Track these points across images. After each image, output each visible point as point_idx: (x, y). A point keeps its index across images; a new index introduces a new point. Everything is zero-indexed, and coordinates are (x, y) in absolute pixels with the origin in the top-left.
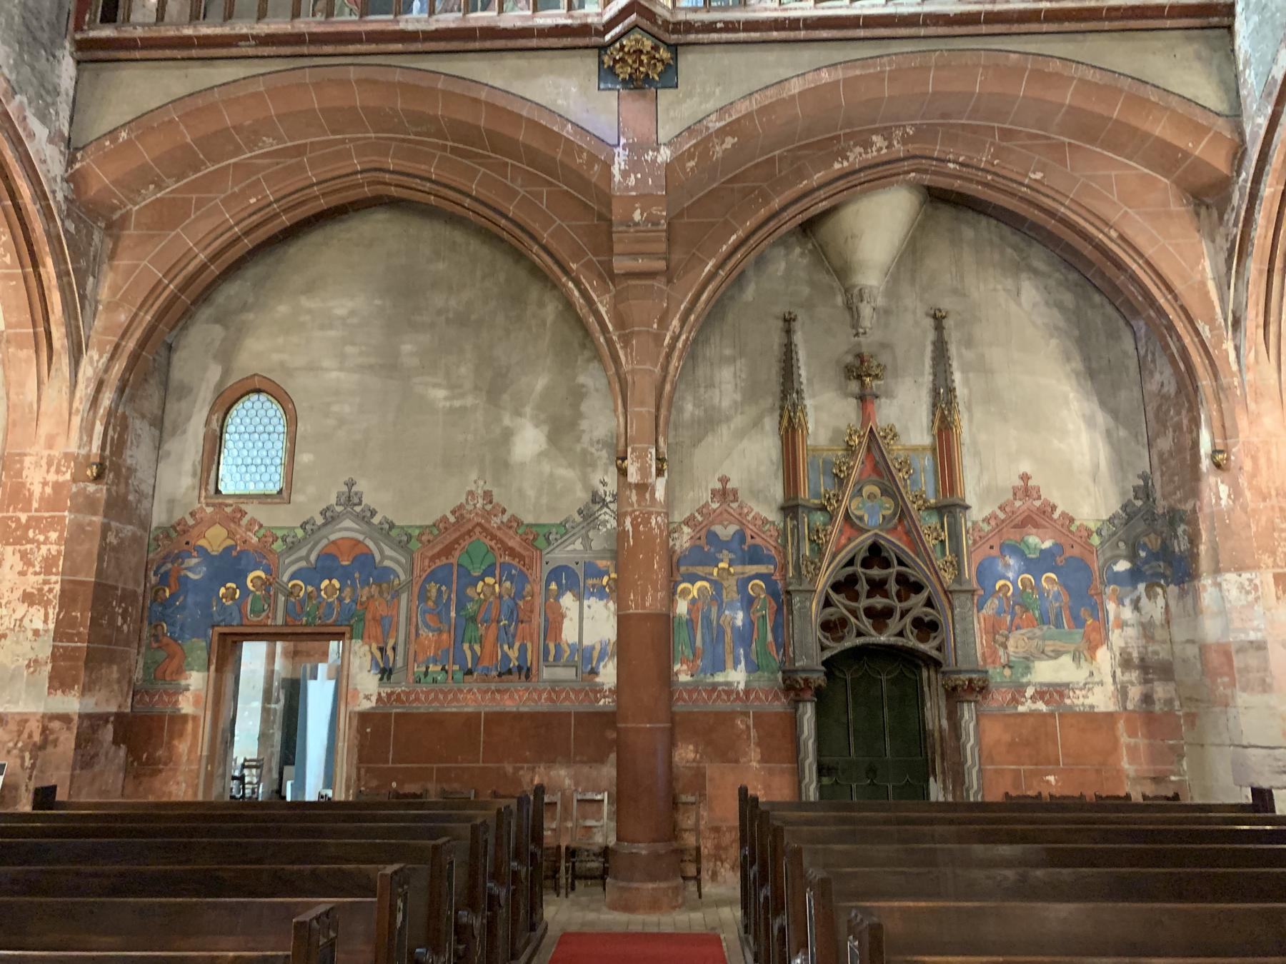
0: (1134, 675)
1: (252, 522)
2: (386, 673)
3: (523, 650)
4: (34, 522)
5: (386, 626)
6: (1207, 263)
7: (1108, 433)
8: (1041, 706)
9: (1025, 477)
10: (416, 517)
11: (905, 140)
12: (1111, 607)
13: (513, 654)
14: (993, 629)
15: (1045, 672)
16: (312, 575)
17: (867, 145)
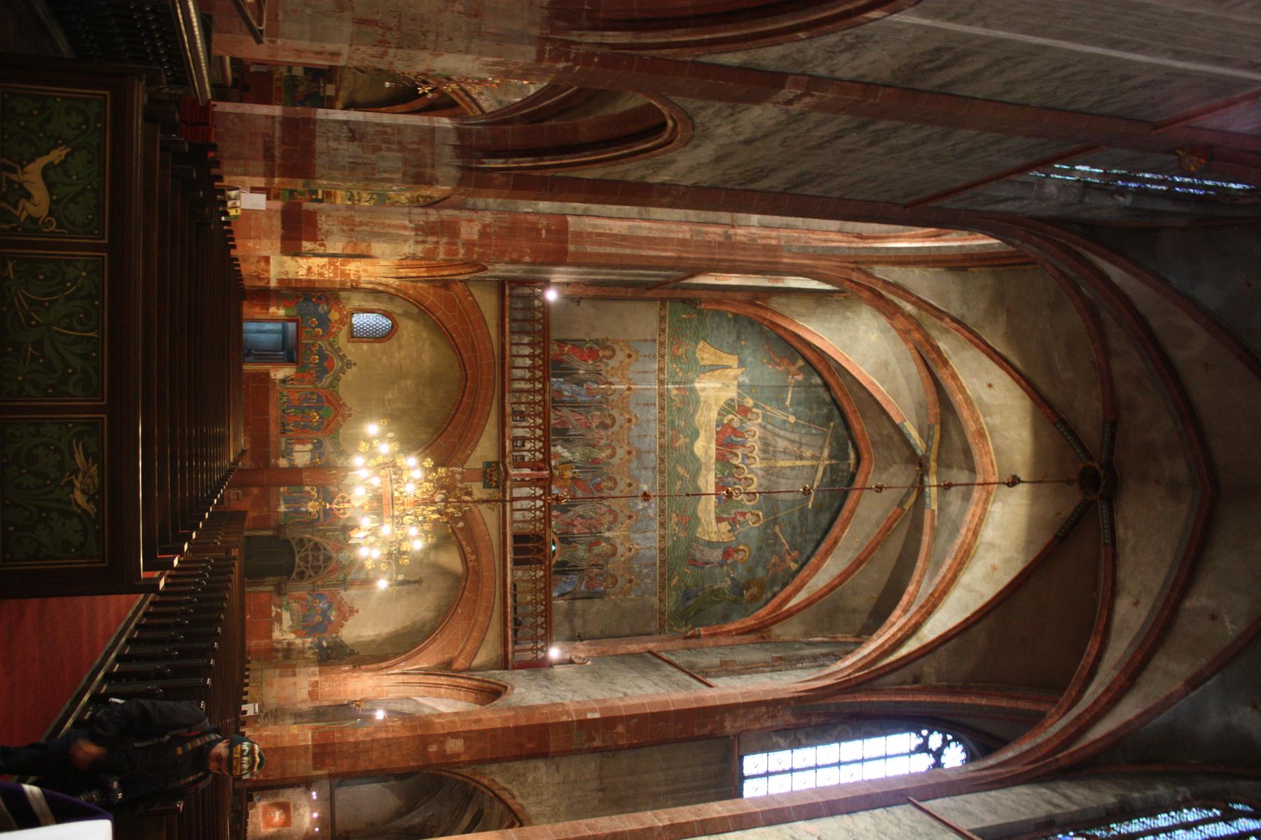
0: (285, 646)
1: (341, 329)
2: (284, 381)
3: (292, 431)
4: (336, 268)
5: (301, 381)
6: (426, 665)
7: (373, 641)
8: (274, 614)
9: (357, 611)
10: (342, 389)
11: (474, 567)
12: (310, 640)
13: (290, 427)
14: (300, 598)
15: (286, 616)
16: (321, 352)
17: (472, 553)
